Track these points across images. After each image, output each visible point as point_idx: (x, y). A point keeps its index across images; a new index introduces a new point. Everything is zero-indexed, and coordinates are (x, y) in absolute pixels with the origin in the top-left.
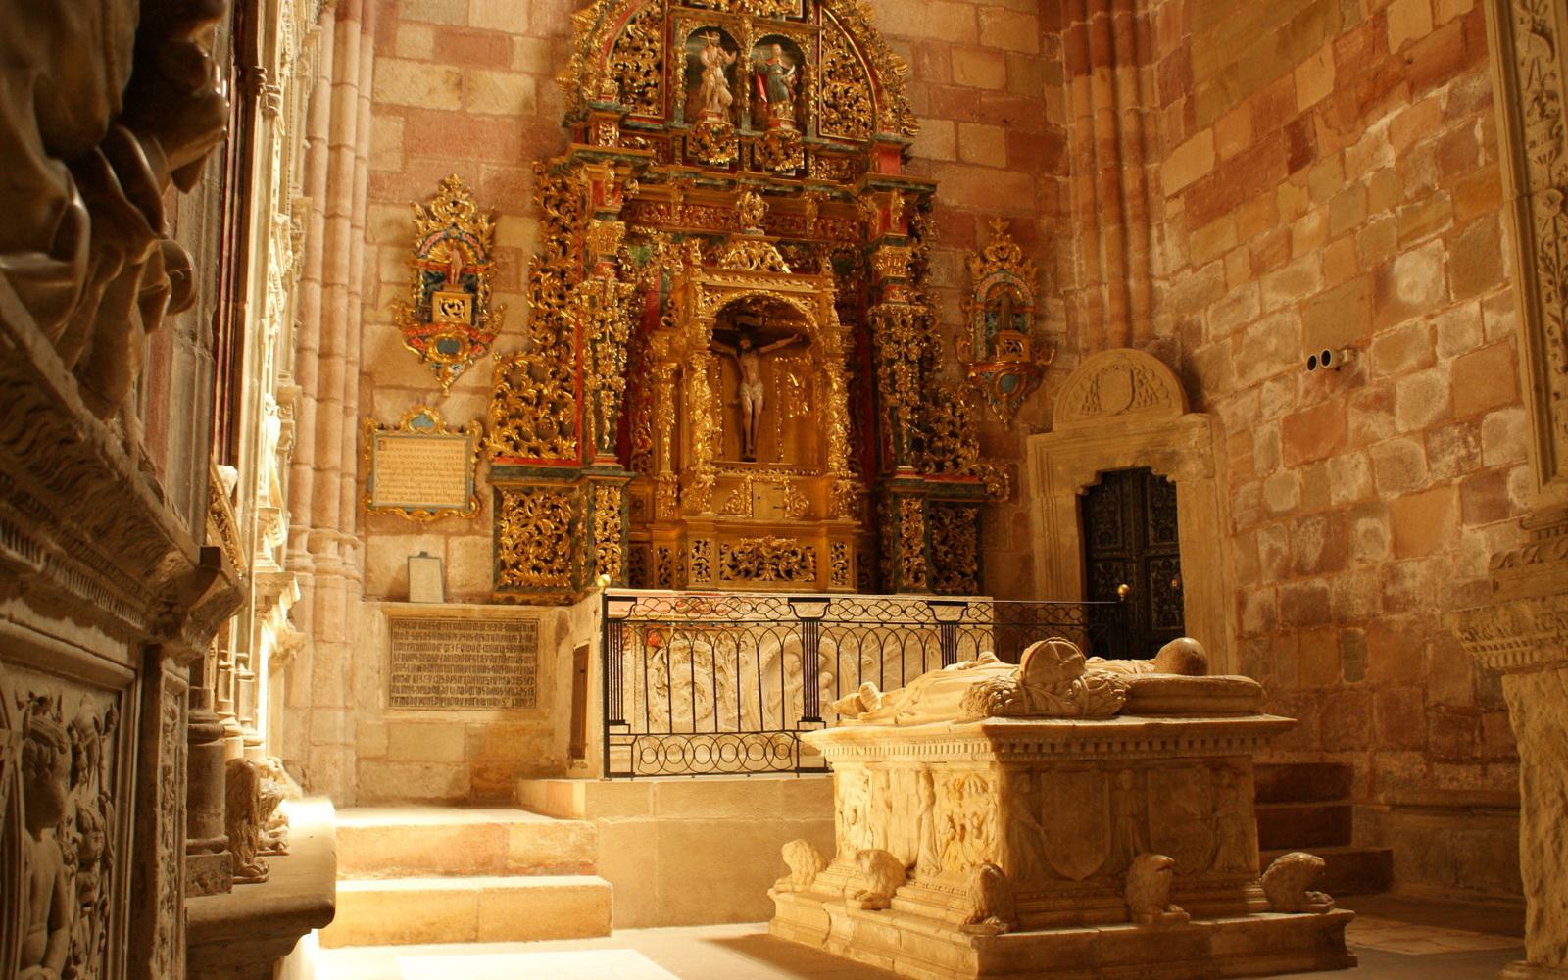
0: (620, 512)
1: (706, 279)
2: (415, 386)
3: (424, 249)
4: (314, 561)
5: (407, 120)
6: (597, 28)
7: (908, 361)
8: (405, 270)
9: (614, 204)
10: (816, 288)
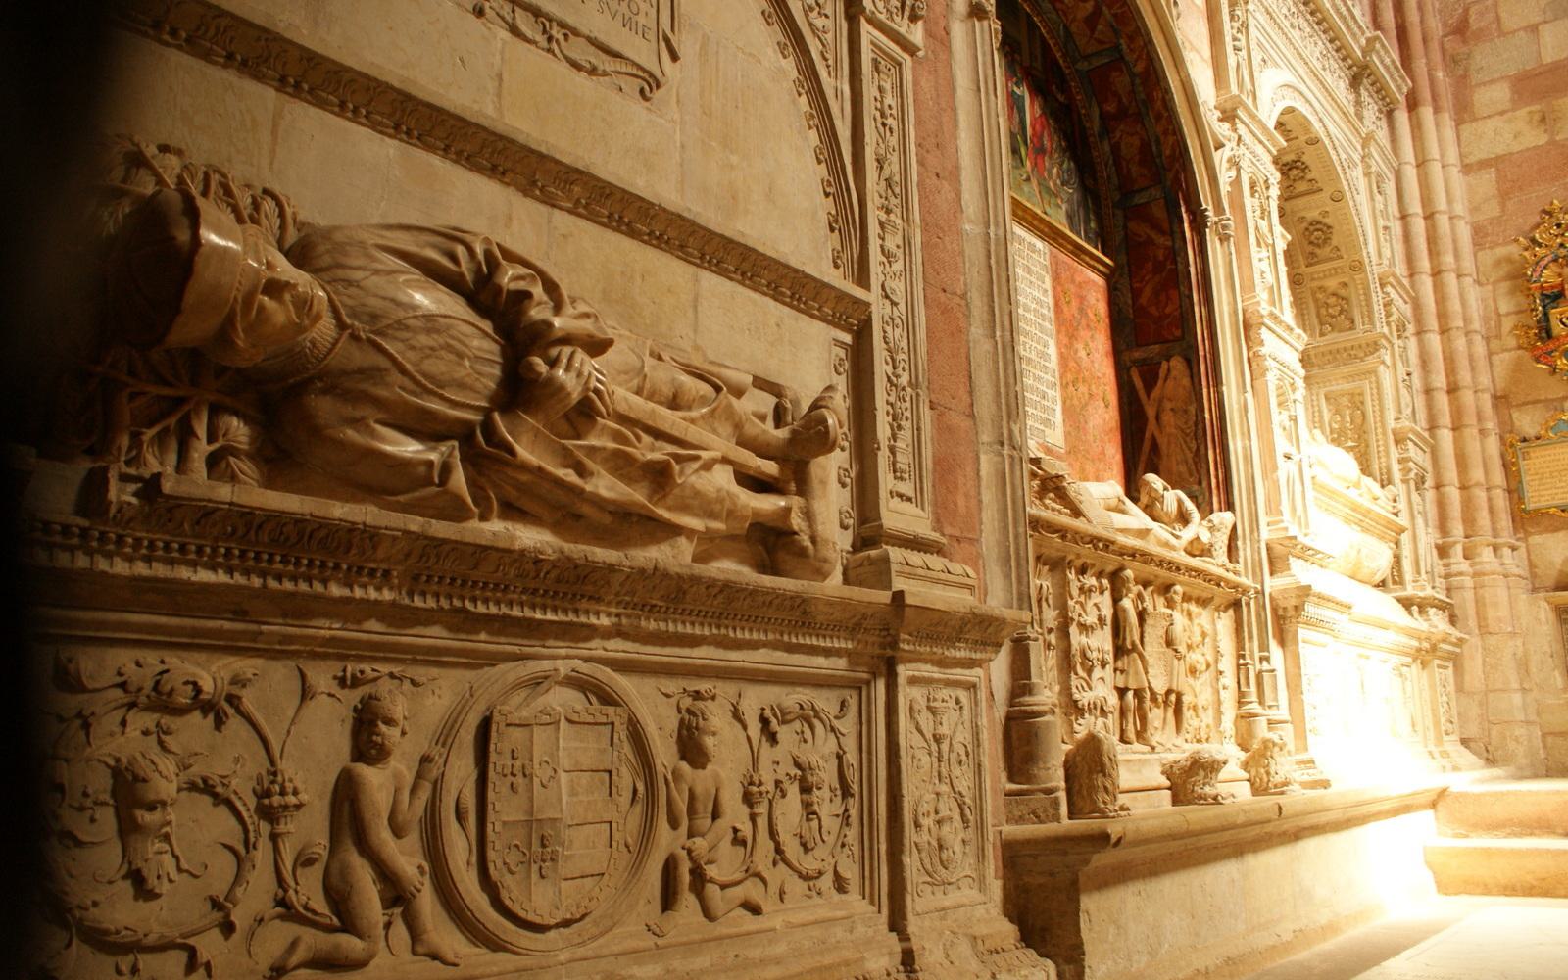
2: (1550, 397)
8: (1522, 299)
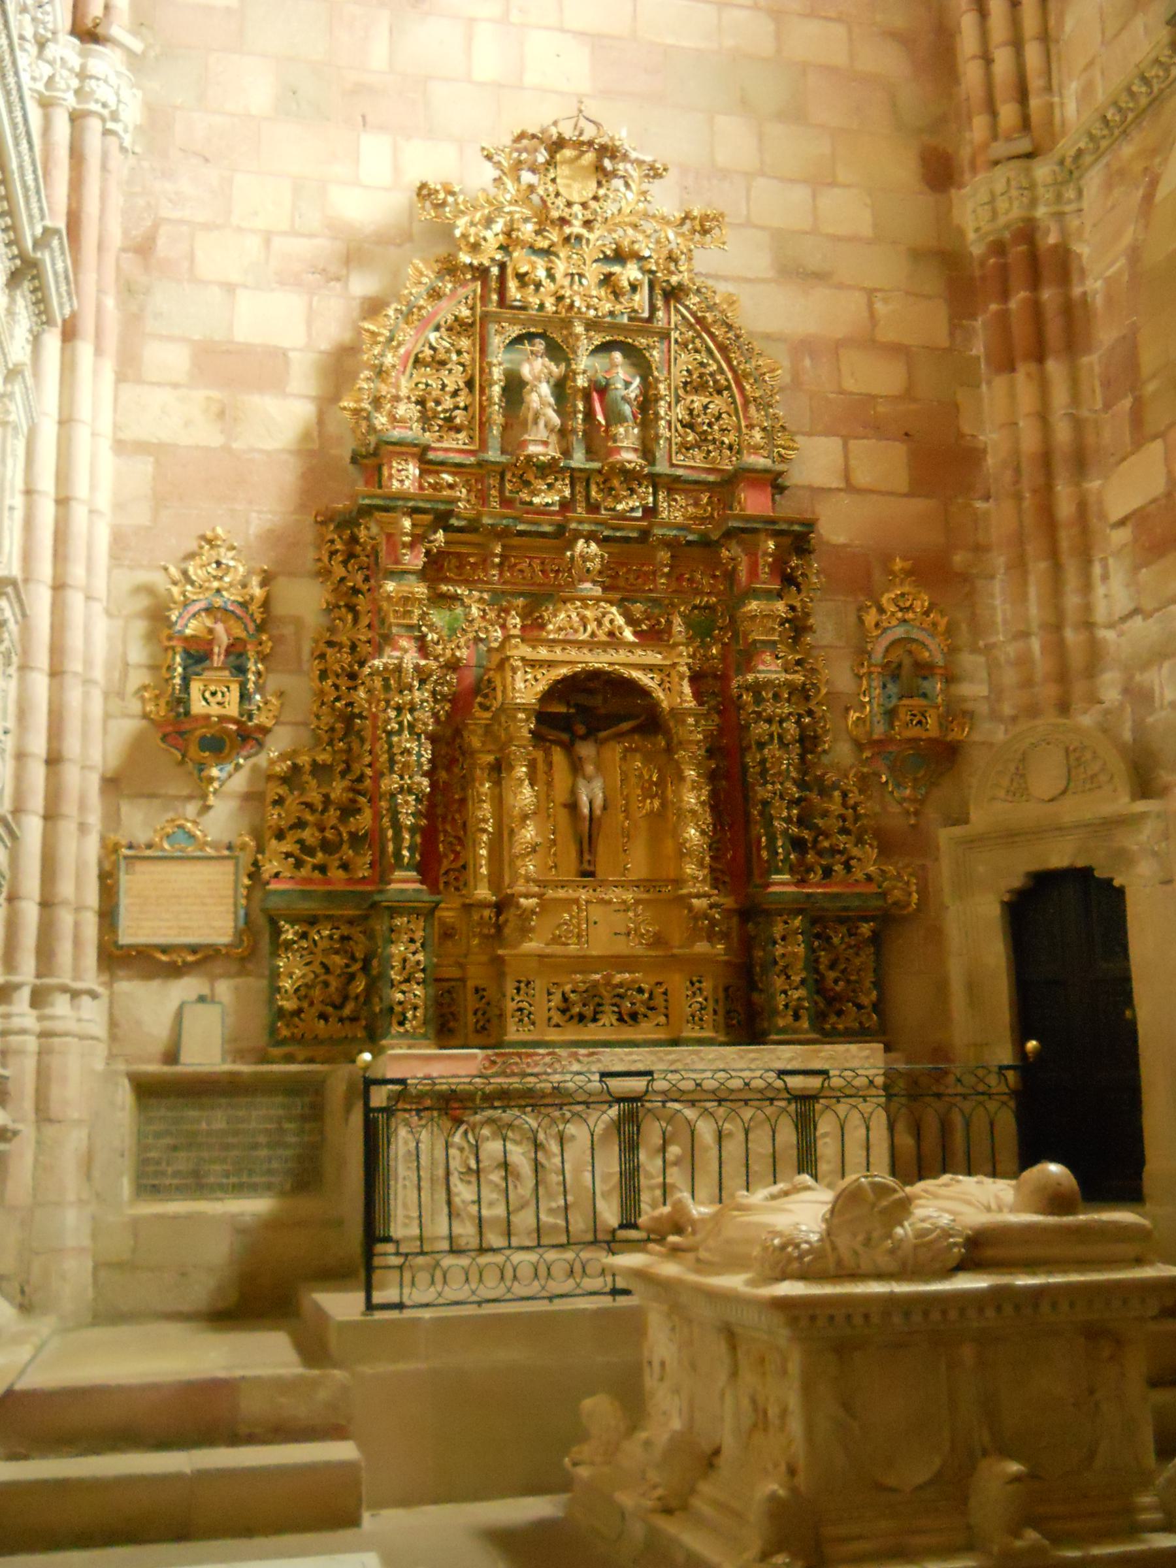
0: (423, 945)
1: (526, 651)
3: (181, 623)
4: (40, 1018)
5: (157, 463)
6: (391, 339)
7: (783, 745)
9: (414, 560)
10: (664, 658)
